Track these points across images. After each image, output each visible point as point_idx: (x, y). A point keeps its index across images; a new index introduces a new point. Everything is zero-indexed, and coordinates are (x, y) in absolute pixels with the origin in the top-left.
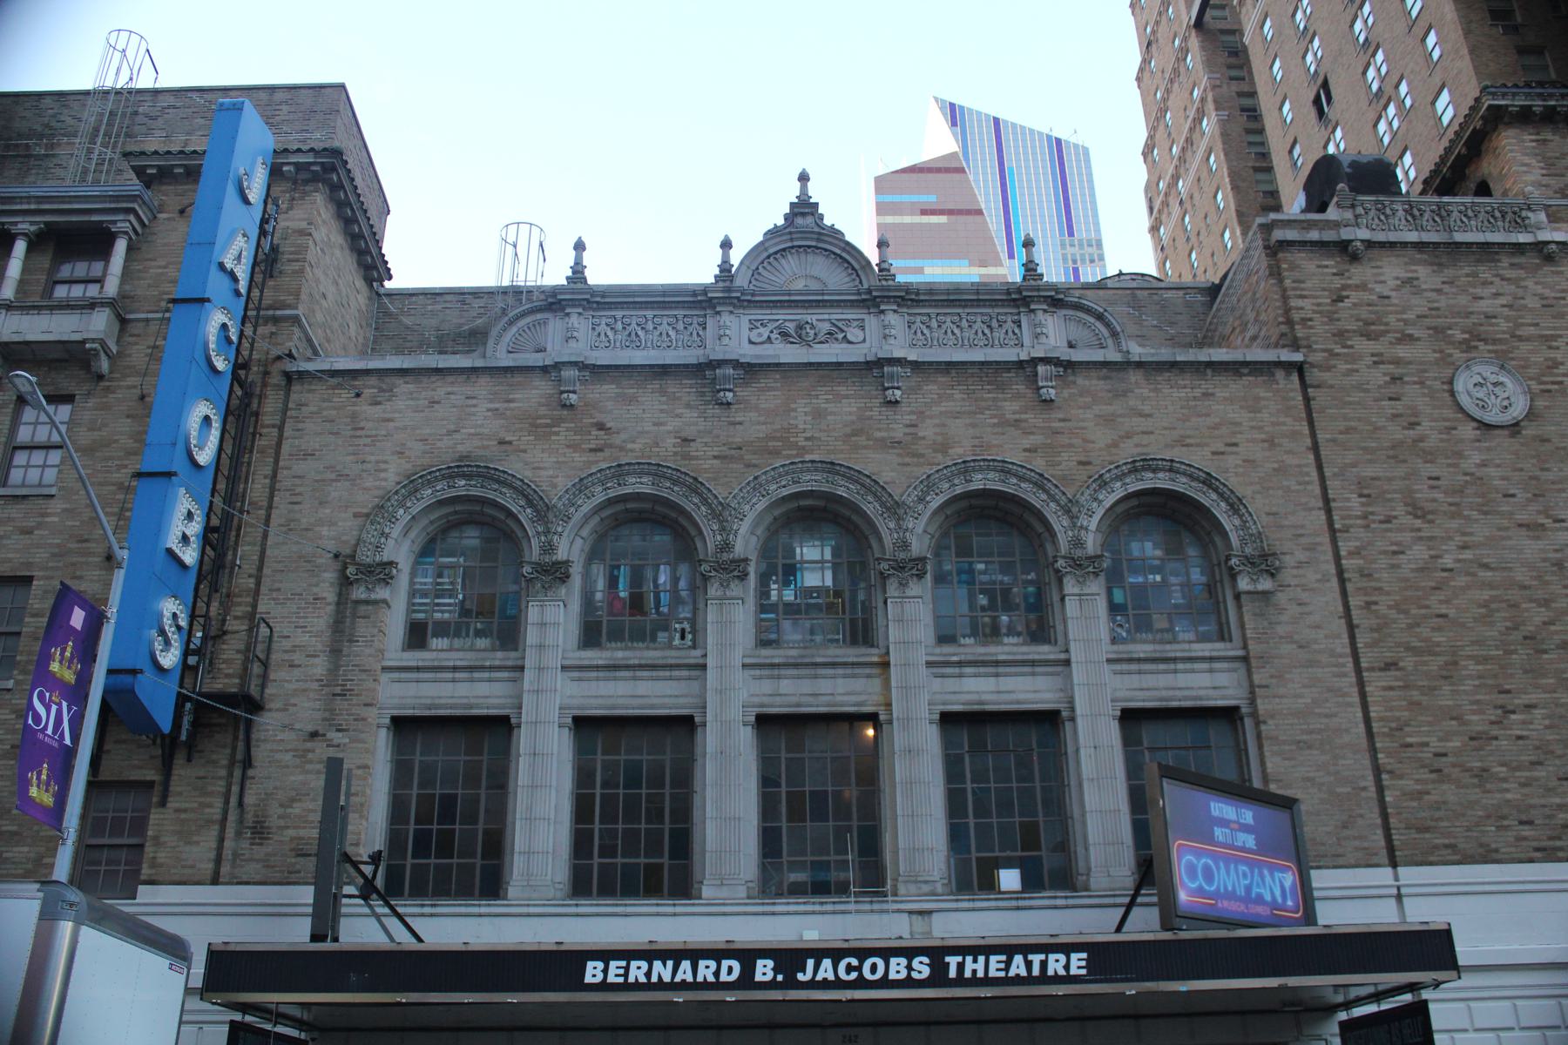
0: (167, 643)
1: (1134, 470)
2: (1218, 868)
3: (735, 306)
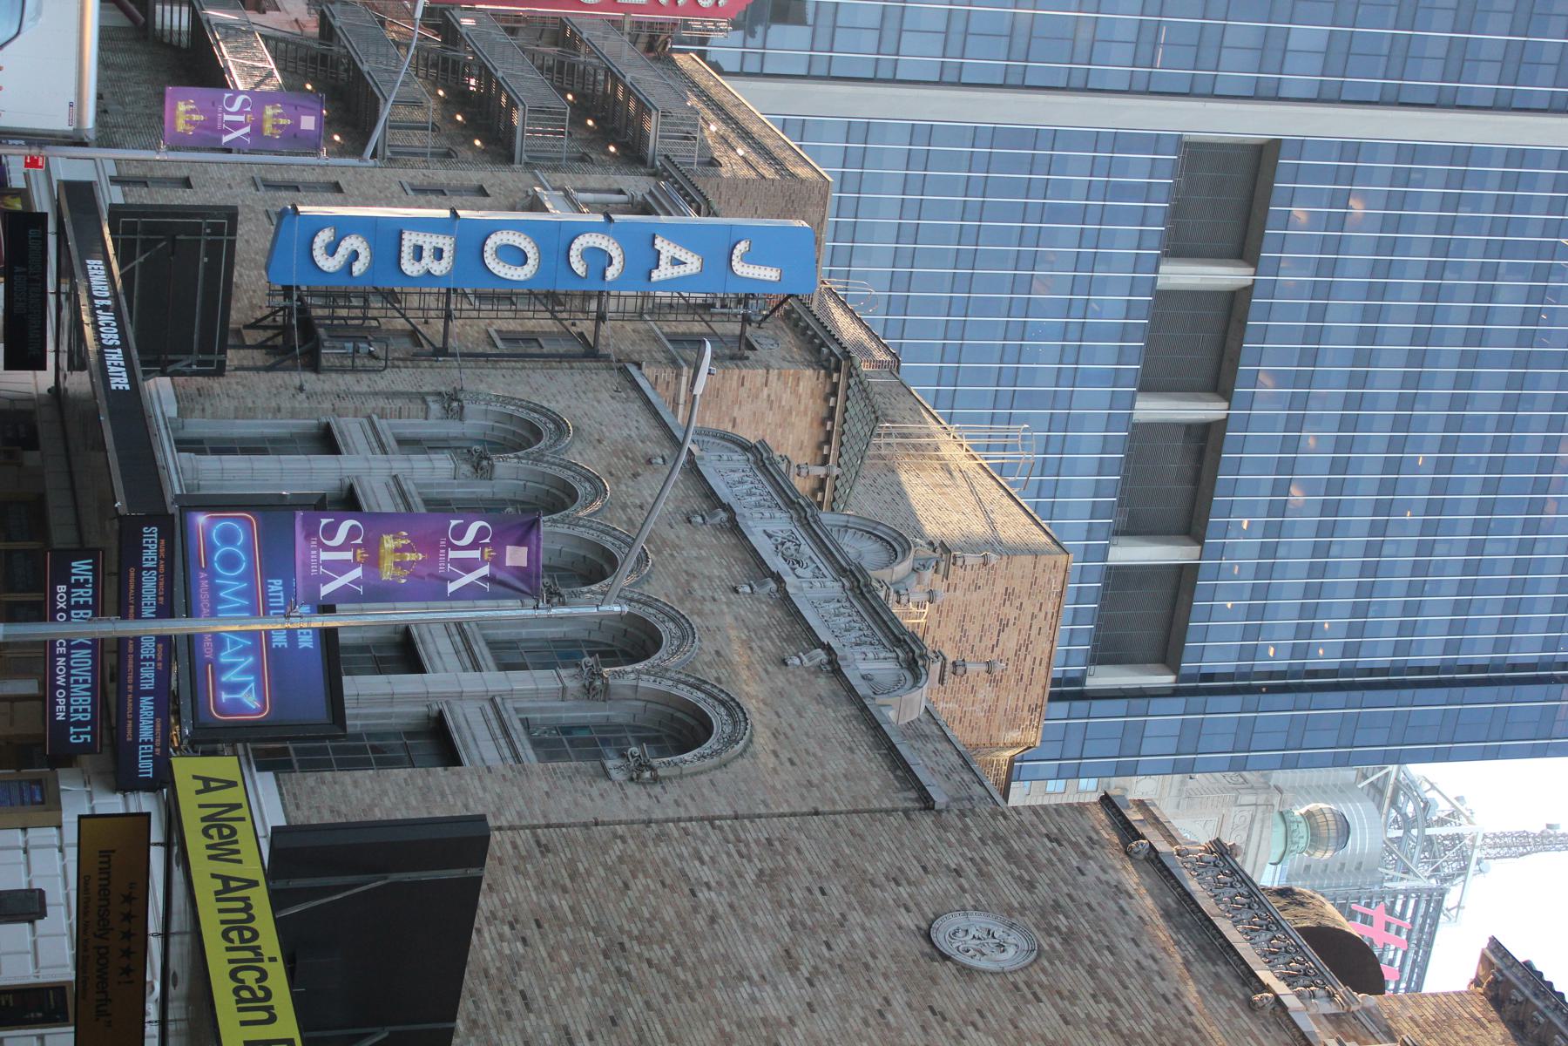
0: (332, 249)
1: (723, 703)
2: (238, 578)
3: (799, 520)
